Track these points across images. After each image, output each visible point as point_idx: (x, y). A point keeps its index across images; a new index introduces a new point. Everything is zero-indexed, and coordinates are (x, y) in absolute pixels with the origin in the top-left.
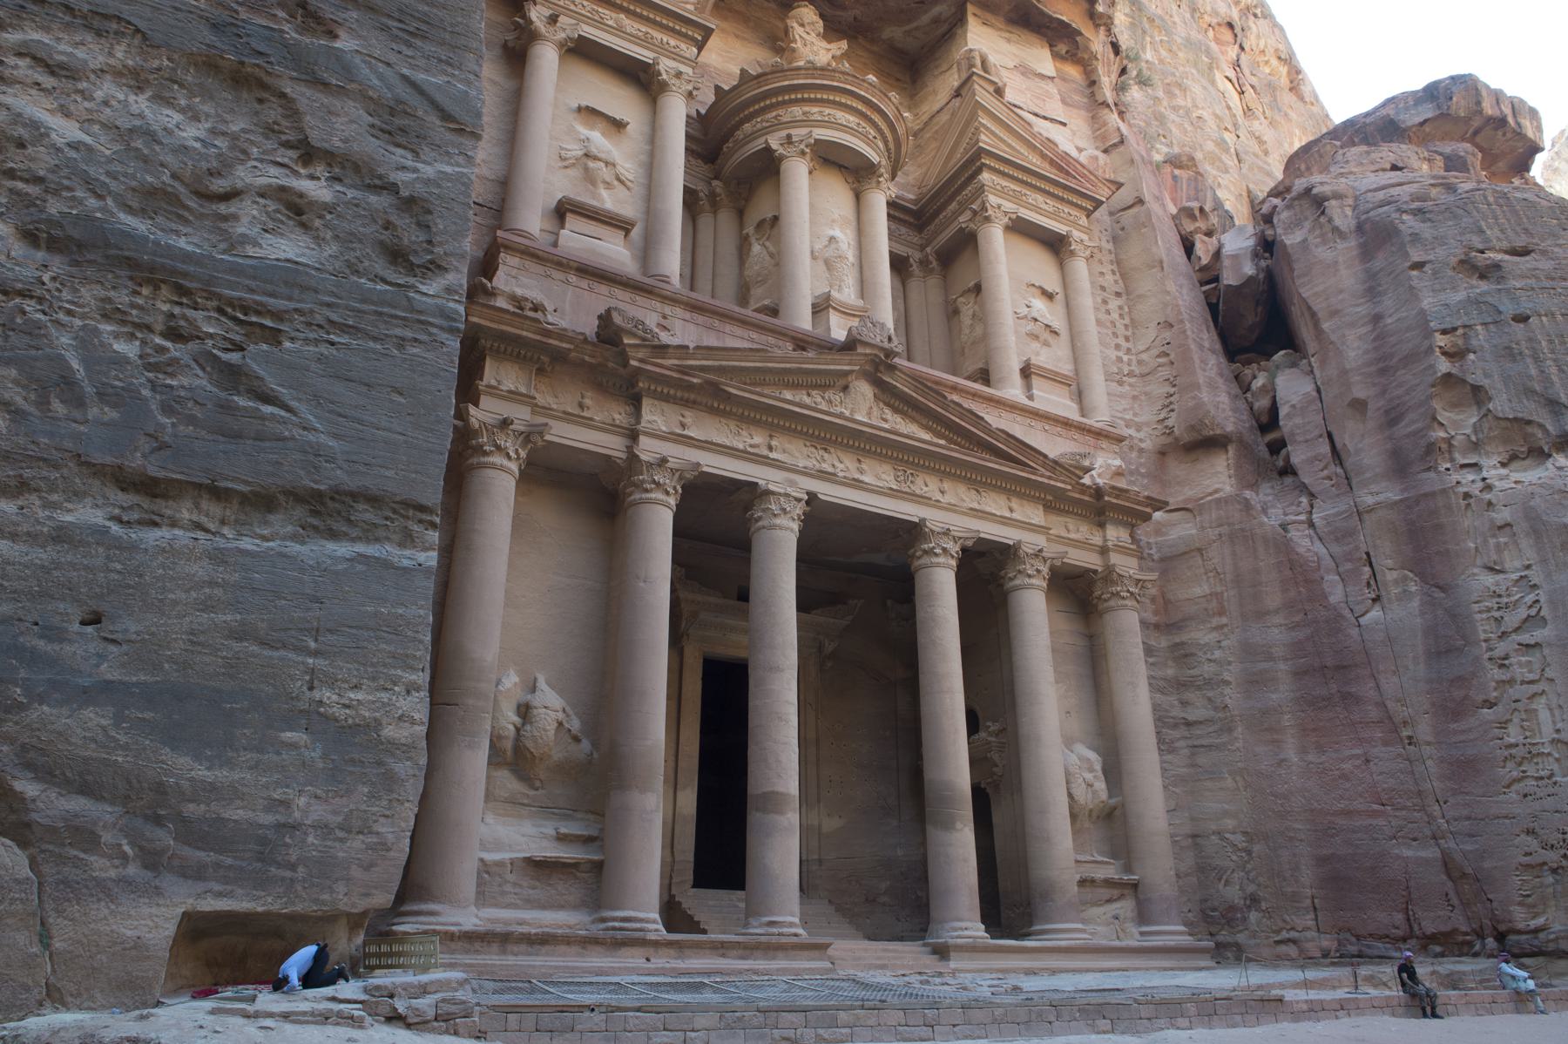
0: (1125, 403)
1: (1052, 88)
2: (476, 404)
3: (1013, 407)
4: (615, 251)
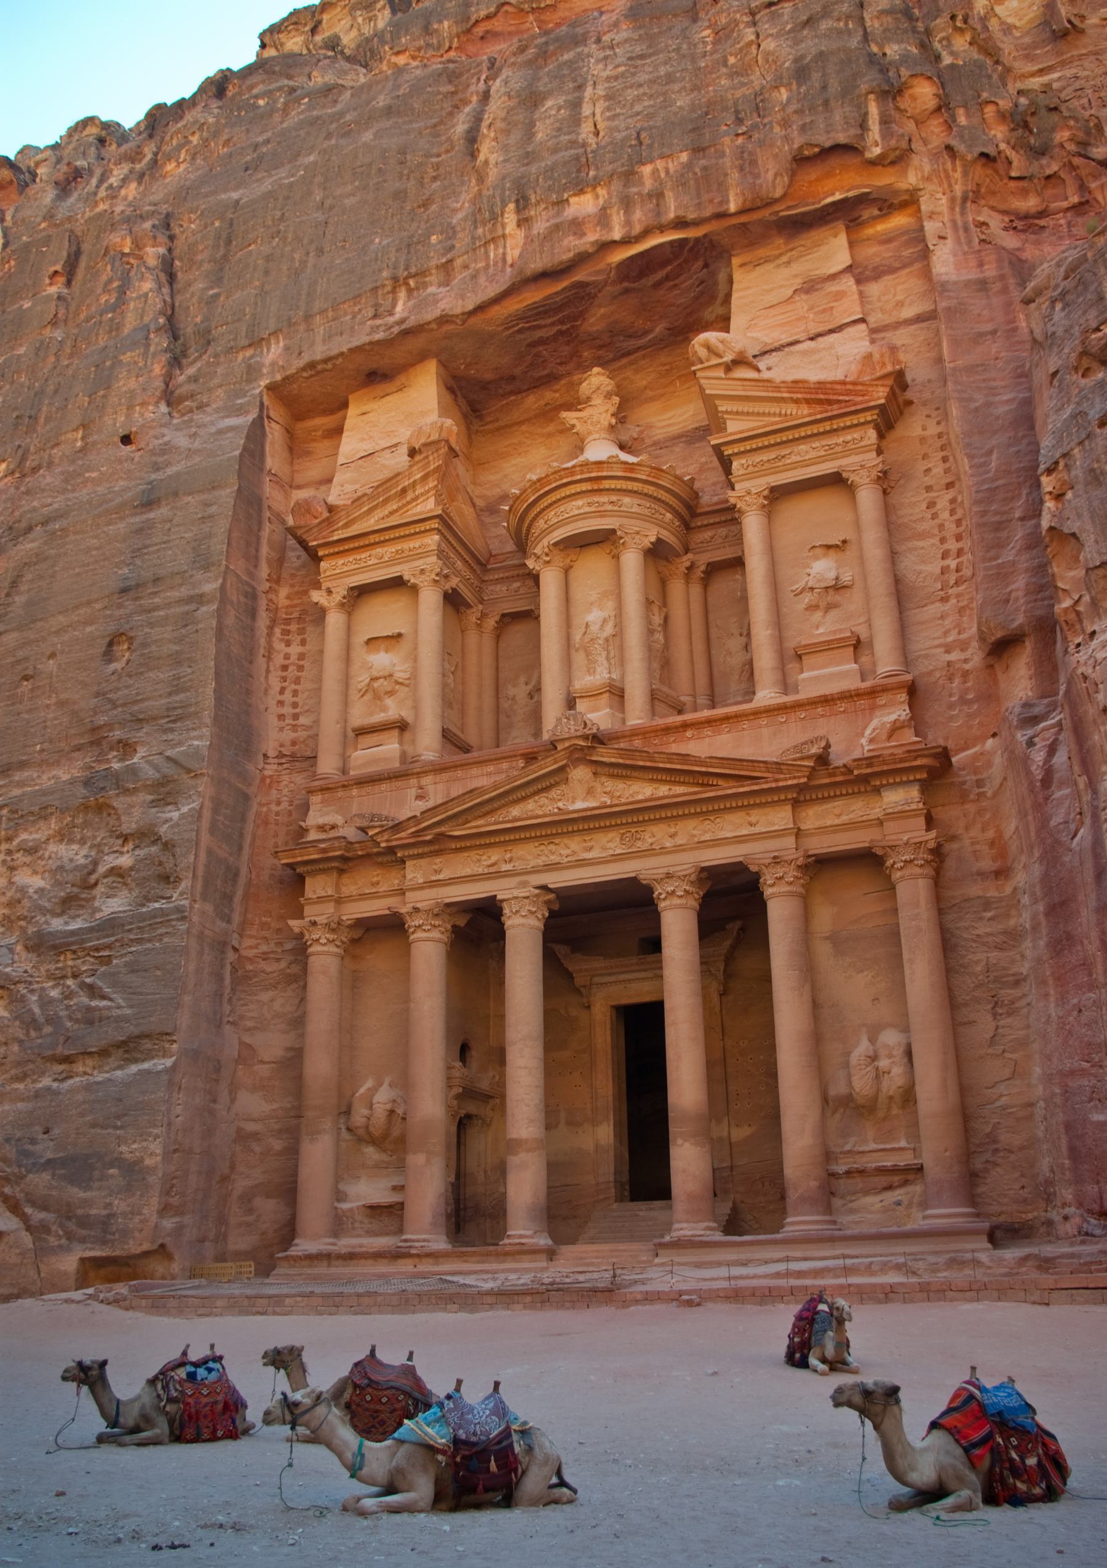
0: (948, 622)
1: (848, 283)
2: (300, 915)
3: (757, 713)
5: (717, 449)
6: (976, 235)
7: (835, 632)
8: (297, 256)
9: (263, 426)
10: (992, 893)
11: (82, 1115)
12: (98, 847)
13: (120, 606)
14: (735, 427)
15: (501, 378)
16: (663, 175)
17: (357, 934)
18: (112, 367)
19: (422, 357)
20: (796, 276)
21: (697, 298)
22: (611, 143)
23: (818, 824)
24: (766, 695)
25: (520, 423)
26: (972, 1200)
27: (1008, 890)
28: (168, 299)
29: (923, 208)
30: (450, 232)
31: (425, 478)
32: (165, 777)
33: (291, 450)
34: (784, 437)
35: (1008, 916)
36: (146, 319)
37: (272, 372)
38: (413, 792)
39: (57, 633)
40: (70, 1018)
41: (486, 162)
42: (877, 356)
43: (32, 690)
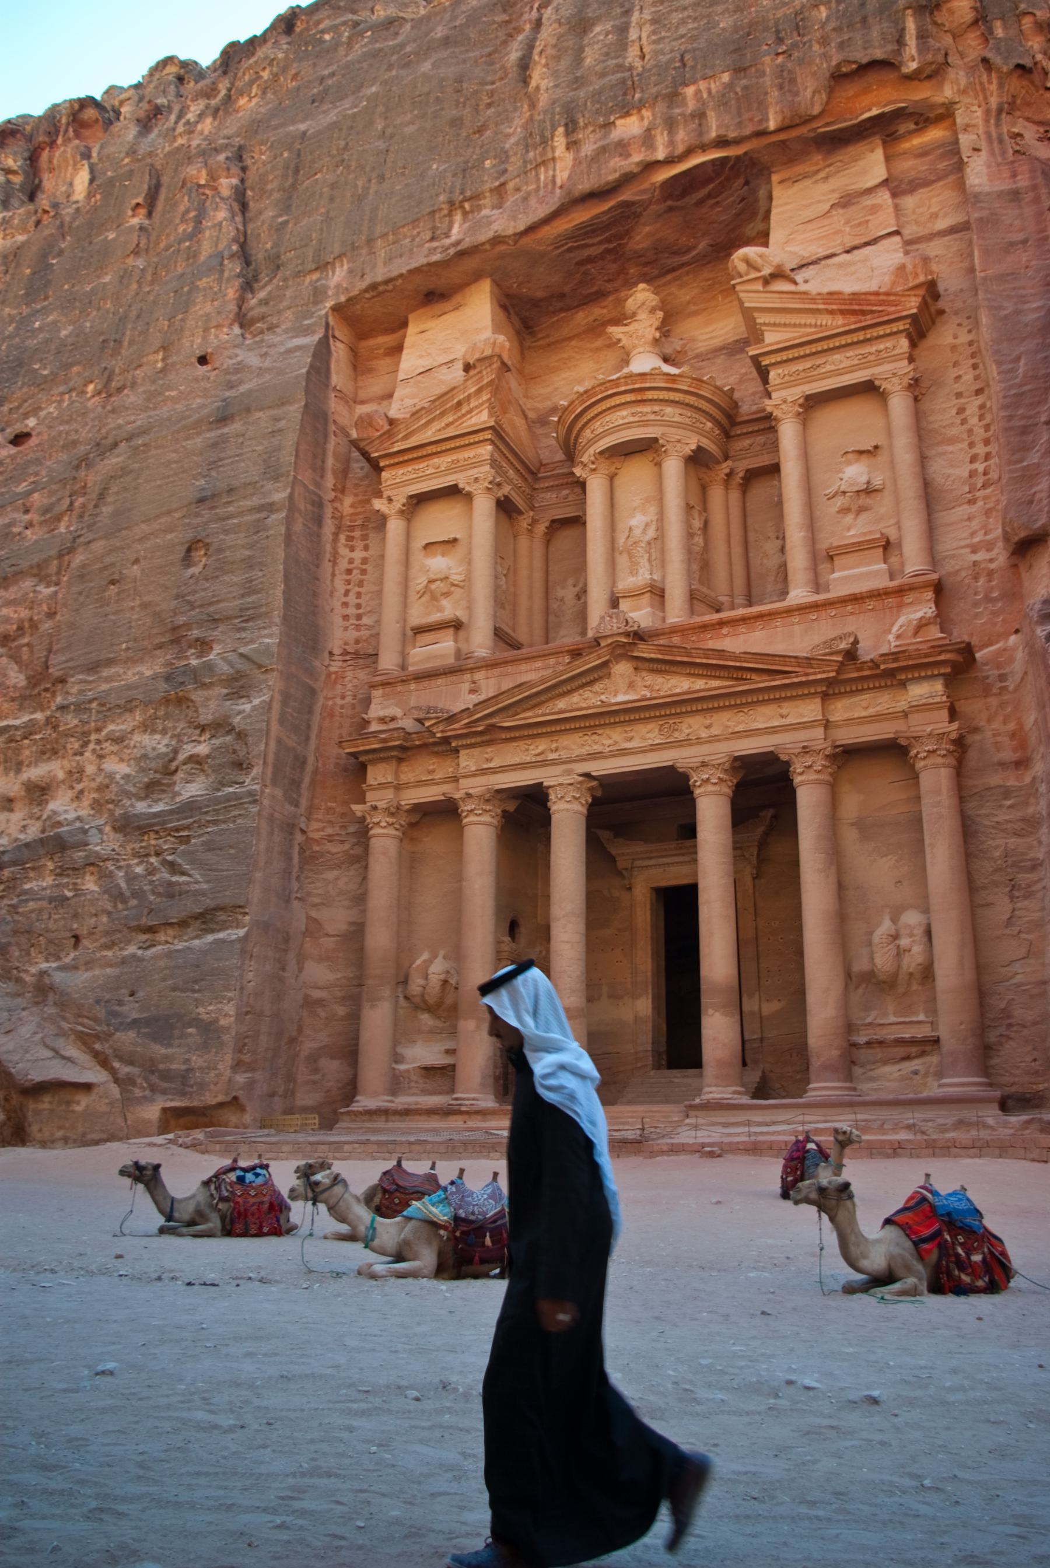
0: (975, 524)
1: (884, 197)
3: (789, 611)
4: (442, 648)
5: (755, 360)
6: (1010, 146)
7: (865, 534)
8: (360, 183)
9: (328, 345)
10: (1012, 782)
11: (164, 979)
12: (178, 737)
13: (197, 515)
14: (772, 338)
15: (552, 296)
16: (705, 96)
17: (414, 818)
18: (190, 292)
19: (477, 277)
20: (833, 191)
21: (738, 215)
22: (656, 66)
23: (846, 716)
24: (799, 594)
25: (570, 339)
26: (985, 1070)
27: (1028, 779)
28: (241, 227)
29: (958, 120)
30: (503, 157)
31: (479, 391)
32: (238, 672)
33: (355, 367)
34: (819, 347)
35: (1027, 804)
36: (221, 247)
37: (337, 294)
38: (467, 686)
39: (141, 540)
40: (153, 893)
41: (538, 88)
42: (909, 267)
43: (118, 594)
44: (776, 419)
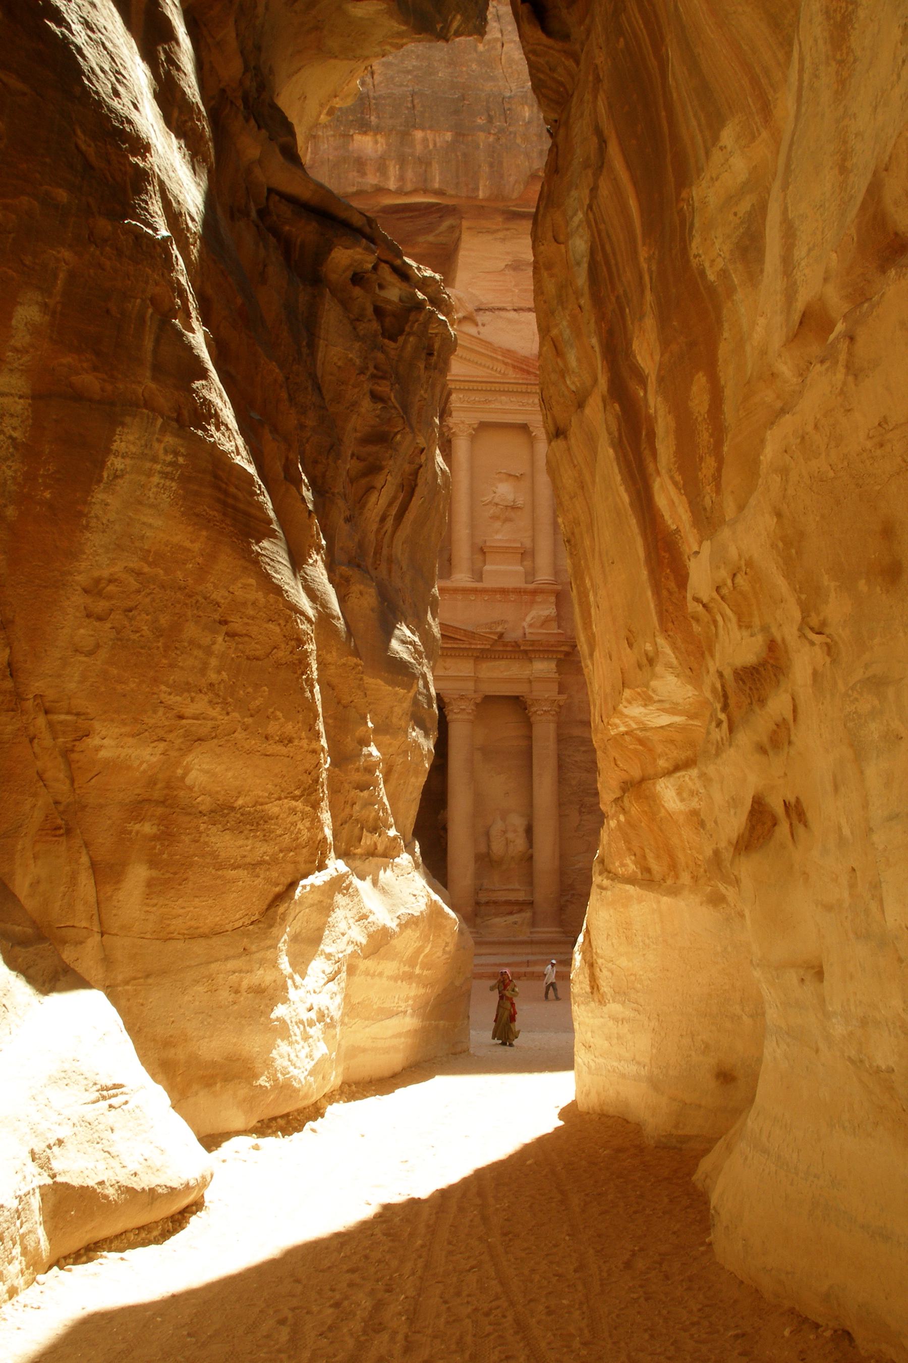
3: (456, 590)
16: (431, 146)
20: (508, 253)
44: (454, 433)
